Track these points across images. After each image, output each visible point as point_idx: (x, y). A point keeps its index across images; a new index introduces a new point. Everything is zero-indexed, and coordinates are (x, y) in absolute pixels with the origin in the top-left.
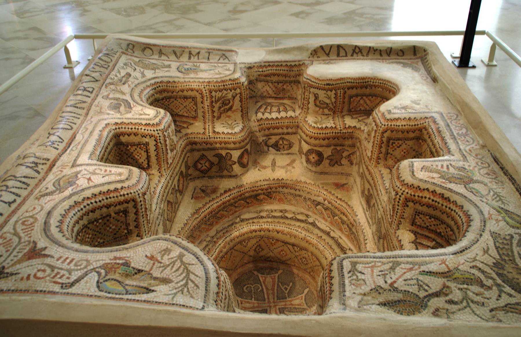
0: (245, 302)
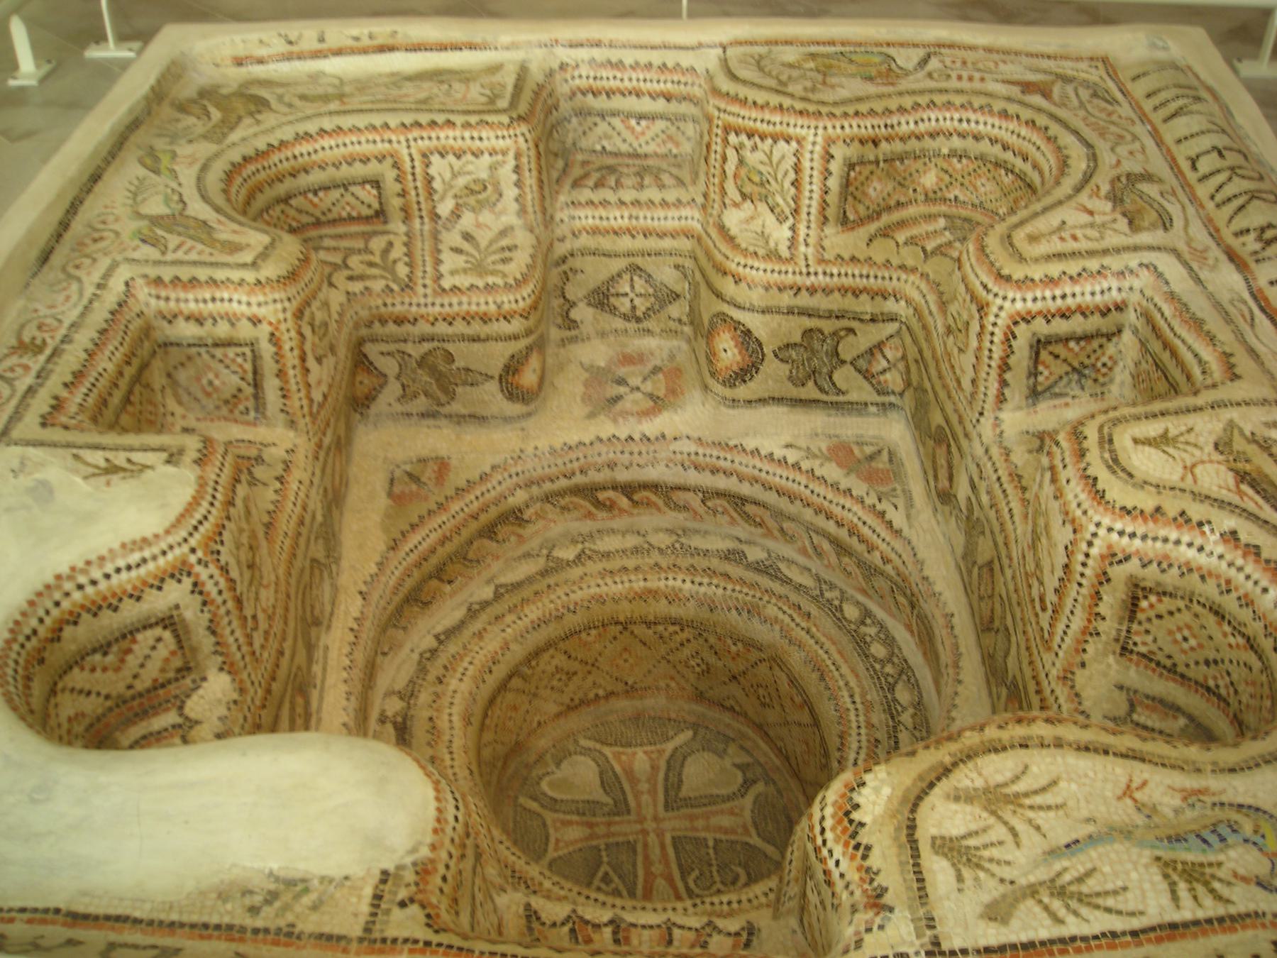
0: (733, 831)
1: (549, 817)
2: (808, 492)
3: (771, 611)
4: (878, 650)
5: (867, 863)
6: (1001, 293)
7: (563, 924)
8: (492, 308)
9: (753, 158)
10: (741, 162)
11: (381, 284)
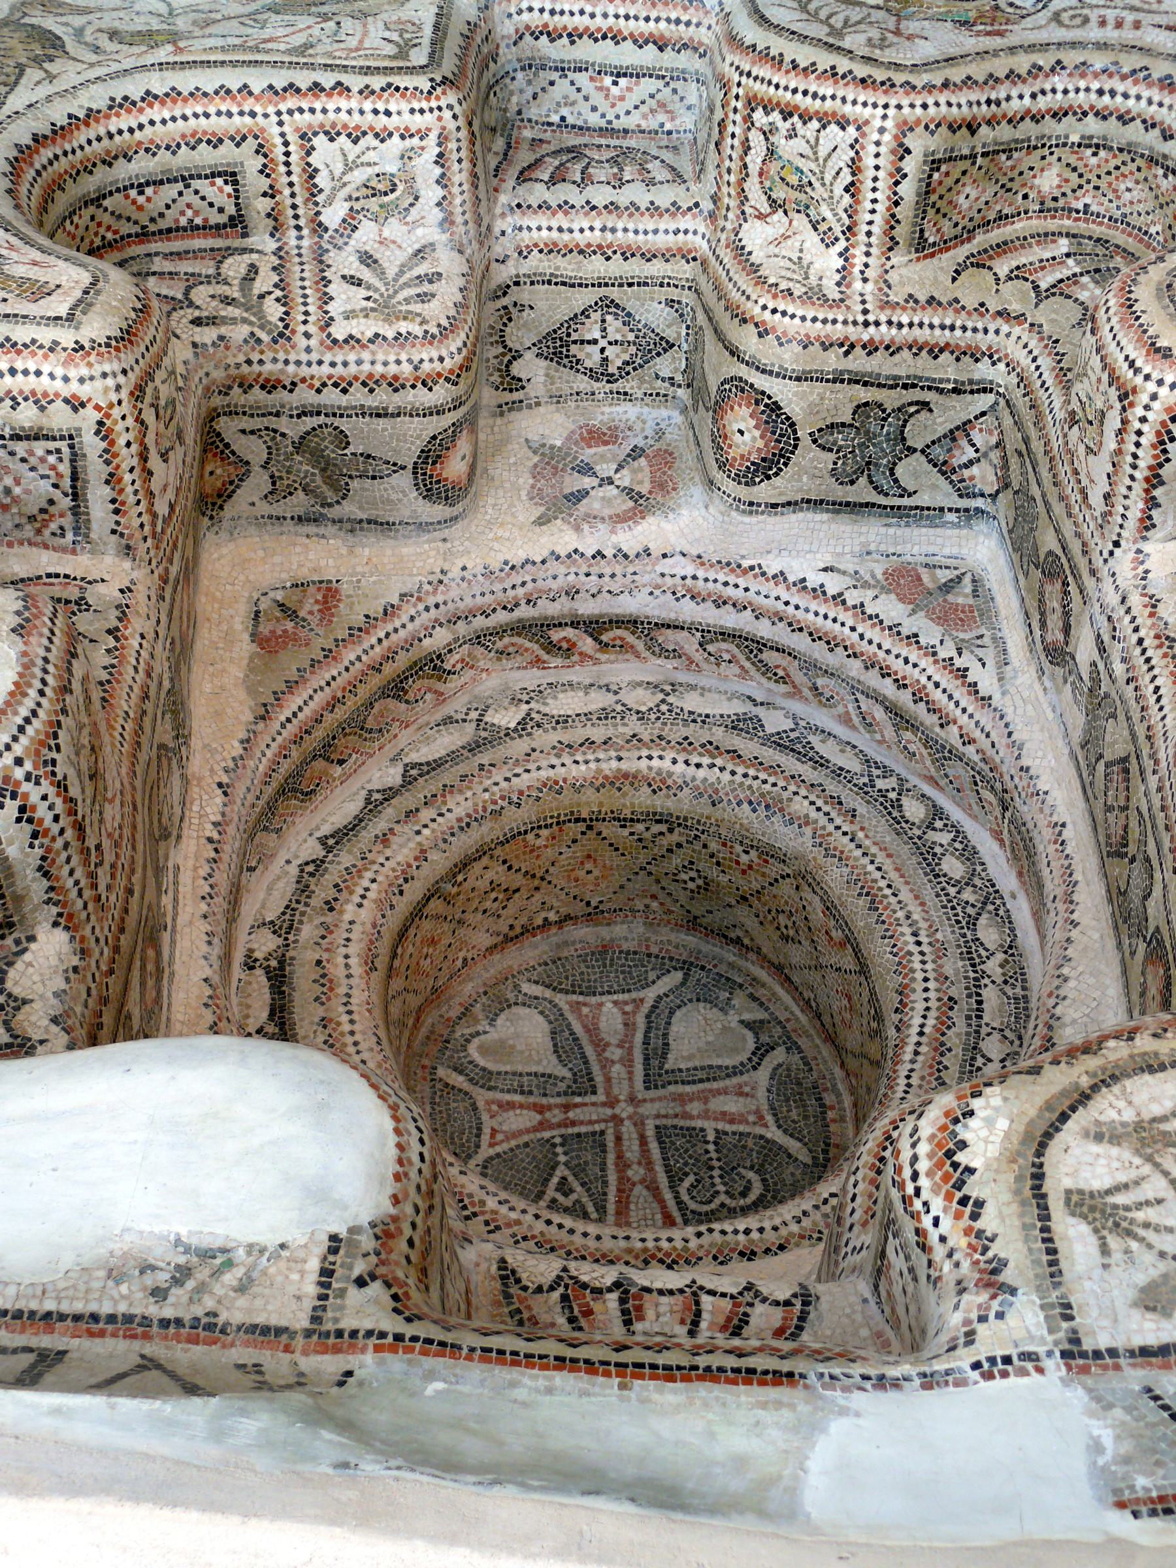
0: (743, 1120)
1: (481, 1096)
2: (855, 636)
3: (800, 806)
4: (953, 867)
5: (978, 1225)
6: (1155, 376)
7: (552, 1288)
8: (406, 368)
9: (788, 149)
10: (771, 152)
11: (245, 330)
